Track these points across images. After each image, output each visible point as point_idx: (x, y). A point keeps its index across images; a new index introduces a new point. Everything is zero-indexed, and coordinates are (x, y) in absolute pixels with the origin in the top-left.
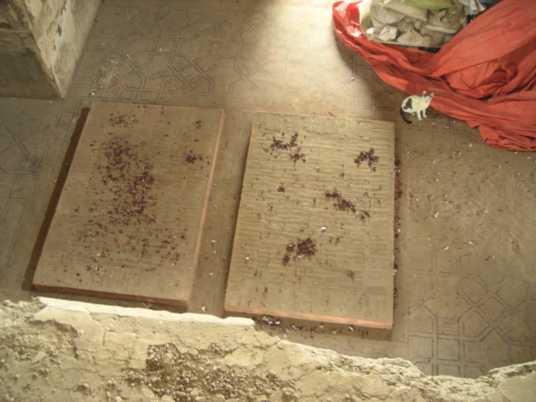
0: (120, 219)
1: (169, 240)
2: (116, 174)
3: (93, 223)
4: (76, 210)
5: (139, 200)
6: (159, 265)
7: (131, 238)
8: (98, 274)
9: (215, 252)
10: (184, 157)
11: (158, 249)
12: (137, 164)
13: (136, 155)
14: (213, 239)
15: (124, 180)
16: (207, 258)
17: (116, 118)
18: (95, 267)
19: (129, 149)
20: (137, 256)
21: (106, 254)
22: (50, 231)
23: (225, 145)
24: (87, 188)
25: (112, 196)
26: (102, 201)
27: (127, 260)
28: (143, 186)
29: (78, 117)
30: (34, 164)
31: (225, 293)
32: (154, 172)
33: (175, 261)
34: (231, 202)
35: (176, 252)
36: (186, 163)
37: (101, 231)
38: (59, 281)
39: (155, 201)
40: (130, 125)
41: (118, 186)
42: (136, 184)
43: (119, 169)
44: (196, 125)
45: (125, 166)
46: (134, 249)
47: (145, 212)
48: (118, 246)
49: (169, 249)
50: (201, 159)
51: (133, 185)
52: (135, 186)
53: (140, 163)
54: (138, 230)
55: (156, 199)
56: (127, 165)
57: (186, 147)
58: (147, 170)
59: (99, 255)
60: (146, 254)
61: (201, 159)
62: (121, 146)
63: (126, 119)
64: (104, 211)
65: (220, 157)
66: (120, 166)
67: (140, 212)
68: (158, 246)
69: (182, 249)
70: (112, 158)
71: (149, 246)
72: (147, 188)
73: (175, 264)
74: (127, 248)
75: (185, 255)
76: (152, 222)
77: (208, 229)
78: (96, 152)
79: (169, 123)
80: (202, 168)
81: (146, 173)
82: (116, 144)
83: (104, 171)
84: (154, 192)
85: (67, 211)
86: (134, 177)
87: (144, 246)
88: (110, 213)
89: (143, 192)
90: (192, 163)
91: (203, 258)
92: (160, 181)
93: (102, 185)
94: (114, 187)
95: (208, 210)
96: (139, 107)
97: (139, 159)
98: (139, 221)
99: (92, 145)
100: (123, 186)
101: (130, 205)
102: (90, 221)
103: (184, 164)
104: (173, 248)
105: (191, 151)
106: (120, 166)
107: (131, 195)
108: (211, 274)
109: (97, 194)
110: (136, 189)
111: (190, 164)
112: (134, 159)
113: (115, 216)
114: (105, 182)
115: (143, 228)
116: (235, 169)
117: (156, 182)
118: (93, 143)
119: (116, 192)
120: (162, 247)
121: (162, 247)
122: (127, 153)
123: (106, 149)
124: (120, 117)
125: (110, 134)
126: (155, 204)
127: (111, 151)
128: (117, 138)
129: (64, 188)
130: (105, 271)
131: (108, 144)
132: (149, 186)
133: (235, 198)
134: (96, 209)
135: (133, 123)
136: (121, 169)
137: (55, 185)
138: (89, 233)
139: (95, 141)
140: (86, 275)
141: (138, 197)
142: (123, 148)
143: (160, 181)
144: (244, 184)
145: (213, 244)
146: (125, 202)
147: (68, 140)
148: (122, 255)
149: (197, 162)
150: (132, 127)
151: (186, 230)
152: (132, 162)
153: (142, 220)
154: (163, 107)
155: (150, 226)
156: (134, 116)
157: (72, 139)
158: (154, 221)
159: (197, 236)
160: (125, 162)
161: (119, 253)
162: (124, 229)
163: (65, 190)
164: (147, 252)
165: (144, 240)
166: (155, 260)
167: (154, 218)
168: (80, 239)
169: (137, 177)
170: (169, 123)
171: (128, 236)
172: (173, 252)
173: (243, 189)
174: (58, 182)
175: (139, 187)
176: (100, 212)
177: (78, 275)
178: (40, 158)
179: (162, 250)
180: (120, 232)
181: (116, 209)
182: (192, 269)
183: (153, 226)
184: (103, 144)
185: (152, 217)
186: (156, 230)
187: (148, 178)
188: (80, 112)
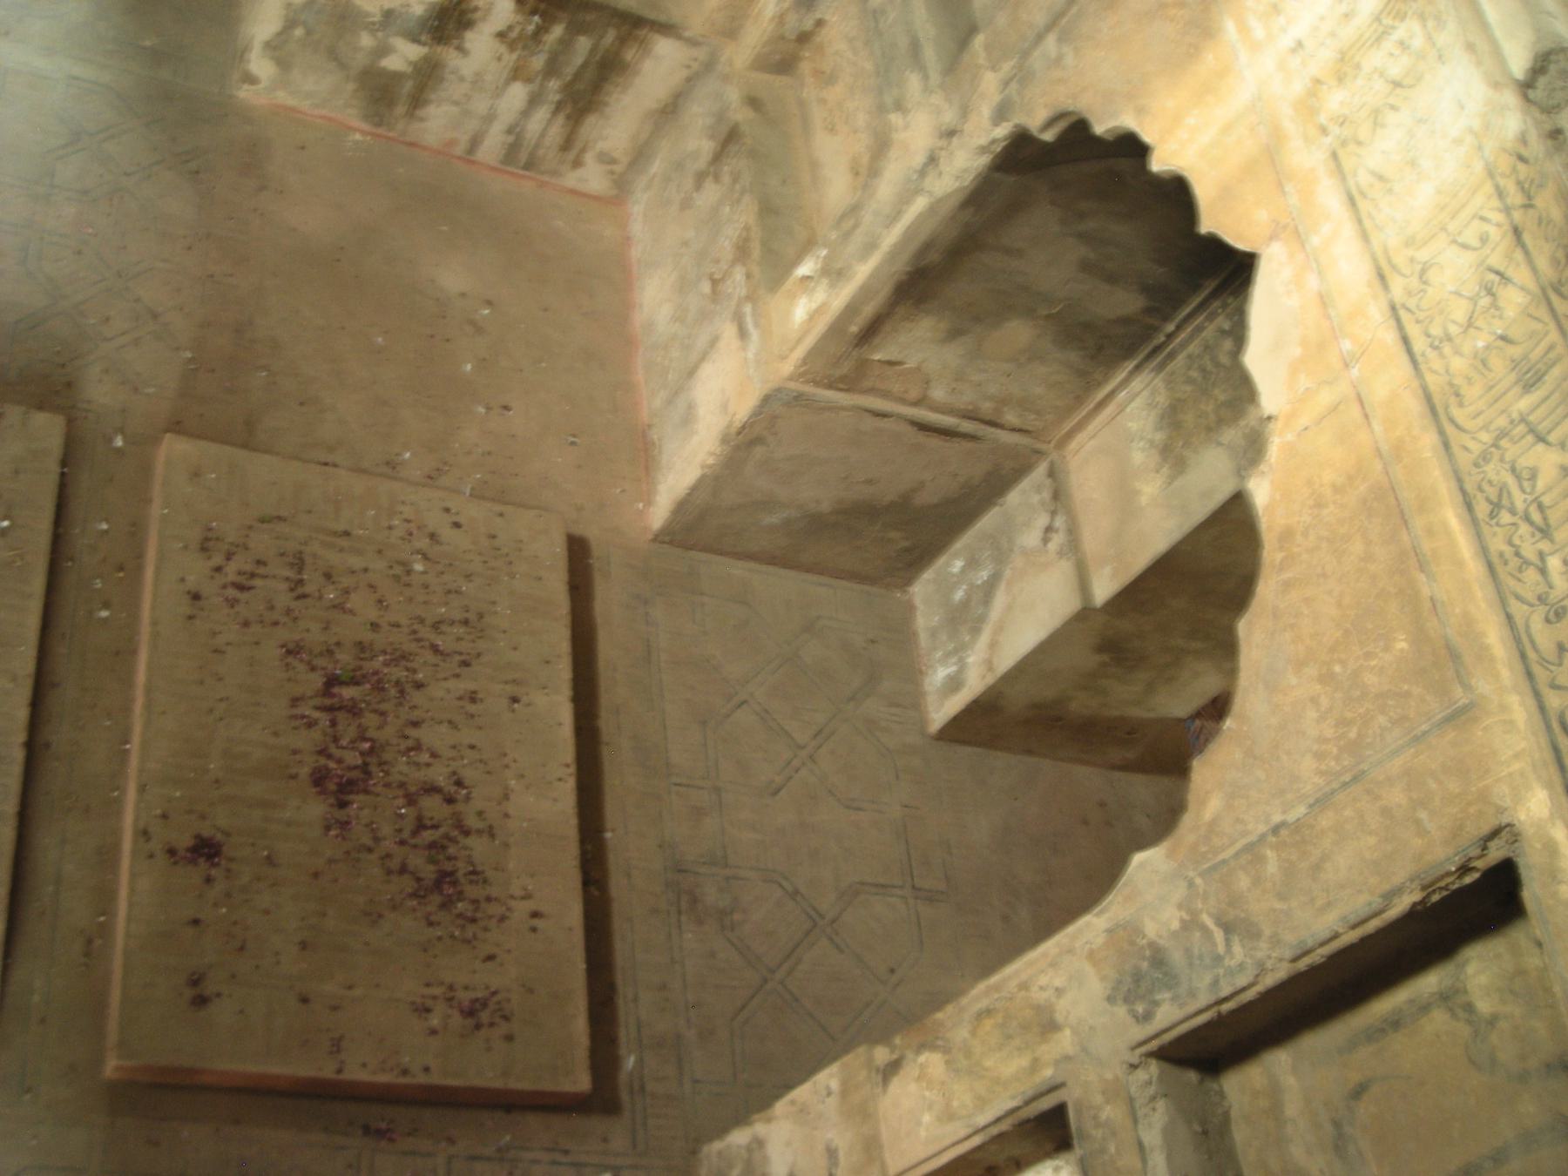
0: (386, 664)
1: (231, 592)
2: (432, 806)
3: (458, 658)
4: (515, 700)
5: (341, 716)
6: (250, 527)
7: (339, 607)
8: (408, 521)
9: (98, 584)
10: (231, 860)
11: (261, 570)
12: (377, 839)
13: (389, 872)
14: (105, 620)
15: (402, 785)
16: (121, 569)
17: (492, 1025)
18: (423, 543)
19: (414, 895)
20: (315, 556)
21: (398, 570)
22: (565, 647)
23: (94, 942)
24: (507, 766)
25: (425, 735)
26: (450, 722)
27: (341, 550)
28: (340, 761)
29: (623, 1077)
30: (694, 901)
31: (63, 474)
32: (317, 809)
33: (210, 535)
34: (59, 735)
35: (209, 558)
36: (219, 837)
37: (426, 632)
38: (501, 515)
39: (298, 711)
40: (437, 991)
41: (417, 764)
42: (365, 769)
43: (429, 823)
44: (209, 988)
45: (415, 833)
46: (328, 576)
47: (317, 681)
48: (371, 586)
49: (231, 569)
50: (172, 852)
51: (374, 769)
52: (366, 764)
53: (367, 840)
54: (326, 629)
55: (295, 717)
56: (406, 835)
57: (228, 895)
58: (341, 815)
59: (419, 567)
60: (291, 559)
61: (172, 852)
62: (443, 906)
63: (457, 1020)
64: (436, 691)
65: (107, 857)
66: (428, 836)
67: (332, 682)
68: (265, 577)
69: (196, 570)
70: (462, 867)
71: (287, 579)
72: (329, 757)
73: (210, 529)
74: (346, 581)
75: (186, 547)
76: (291, 646)
77: (125, 653)
78: (518, 892)
79: (305, 1000)
80: (164, 816)
81: (343, 805)
82: (460, 915)
83: (472, 822)
84: (305, 740)
85: (540, 700)
86: (378, 795)
87: (301, 582)
88: (419, 686)
89: (336, 740)
90: (198, 837)
91: (131, 567)
92: (294, 777)
93: (469, 775)
94: (428, 765)
95: (127, 709)
96: (427, 1070)
97: (374, 857)
98: (330, 652)
99: (535, 915)
100: (405, 769)
101: (368, 704)
102: (466, 664)
103: (228, 834)
104: (218, 569)
105: (209, 880)
106: (428, 836)
107: (371, 733)
108: (105, 526)
109: (472, 747)
110: (362, 754)
111: (206, 833)
112: (388, 856)
113: (398, 673)
114: (459, 783)
115: (314, 635)
116: (49, 849)
117: (305, 771)
118: (536, 922)
119: (418, 747)
120: (253, 575)
121: (253, 575)
122: (419, 880)
123: (489, 899)
124: (478, 1027)
125: (491, 958)
126: (295, 701)
127: (472, 891)
128: (469, 942)
129: (573, 769)
130: (390, 528)
131: (490, 917)
132: (323, 761)
133: (47, 745)
134: (460, 698)
135: (429, 1003)
136: (420, 826)
137: (609, 825)
138: (460, 630)
139: (534, 930)
140: (436, 521)
141: (348, 730)
142: (436, 899)
143: (294, 777)
144: (19, 755)
145: (106, 605)
146: (383, 714)
147: (624, 992)
148: (356, 562)
149: (184, 841)
150: (428, 985)
151: (191, 617)
152: (388, 845)
153: (321, 654)
154: (339, 1071)
155: (297, 637)
156: (433, 1032)
157: (612, 987)
158: (289, 652)
159: (156, 598)
160: (415, 846)
161: (366, 570)
162: (367, 636)
163: (568, 766)
164: (292, 565)
165: (304, 596)
166: (262, 542)
167: (290, 659)
168: (481, 616)
169: (366, 792)
170: (305, 1000)
171: (352, 612)
172: (218, 560)
173: (21, 737)
174: (600, 830)
175: (353, 758)
176: (448, 691)
177: (457, 525)
178: (684, 918)
179: (248, 568)
180: (375, 626)
181: (402, 692)
182: (156, 510)
183: (284, 634)
184: (502, 919)
185: (295, 663)
186: (276, 624)
187: (332, 787)
188: (625, 1096)
